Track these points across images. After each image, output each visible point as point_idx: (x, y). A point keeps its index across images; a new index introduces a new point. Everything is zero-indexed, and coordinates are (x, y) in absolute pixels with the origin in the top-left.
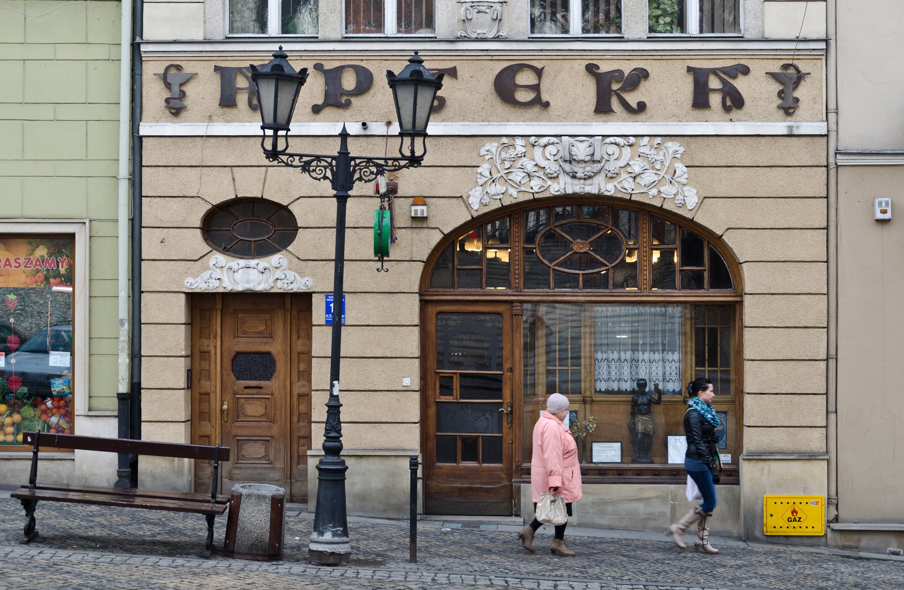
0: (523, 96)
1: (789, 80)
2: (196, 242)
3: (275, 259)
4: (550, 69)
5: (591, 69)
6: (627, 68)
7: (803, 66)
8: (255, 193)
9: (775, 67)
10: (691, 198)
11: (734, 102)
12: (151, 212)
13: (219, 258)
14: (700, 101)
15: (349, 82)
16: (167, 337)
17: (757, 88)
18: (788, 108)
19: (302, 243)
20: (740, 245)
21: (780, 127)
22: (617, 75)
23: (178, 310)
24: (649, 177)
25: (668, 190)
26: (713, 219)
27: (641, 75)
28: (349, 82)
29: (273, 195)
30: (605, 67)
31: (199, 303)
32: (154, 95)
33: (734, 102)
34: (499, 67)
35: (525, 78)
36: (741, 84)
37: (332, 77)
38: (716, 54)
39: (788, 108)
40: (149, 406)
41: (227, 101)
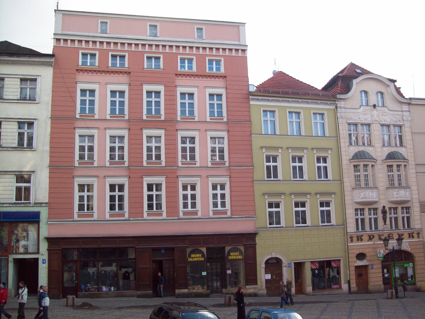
0: (391, 238)
1: (418, 234)
2: (355, 259)
3: (365, 261)
4: (394, 234)
5: (398, 234)
6: (402, 233)
7: (420, 232)
8: (362, 252)
9: (417, 232)
10: (410, 249)
11: (413, 237)
12: (350, 255)
13: (358, 261)
14: (409, 237)
15: (372, 237)
16: (353, 272)
17: (415, 235)
18: (418, 237)
19: (368, 258)
20: (415, 255)
21: (418, 240)
22: (401, 234)
23: (354, 269)
24: (405, 247)
25: (407, 248)
26: (412, 252)
27: (403, 234)
28: (372, 237)
29: (364, 252)
30: (399, 233)
31: (356, 267)
32: (349, 240)
33: (413, 237)
34: (388, 234)
35: (391, 235)
36: (414, 235)
37: (370, 236)
38: (410, 231)
39: (418, 237)
40: (351, 282)
41: (358, 240)
